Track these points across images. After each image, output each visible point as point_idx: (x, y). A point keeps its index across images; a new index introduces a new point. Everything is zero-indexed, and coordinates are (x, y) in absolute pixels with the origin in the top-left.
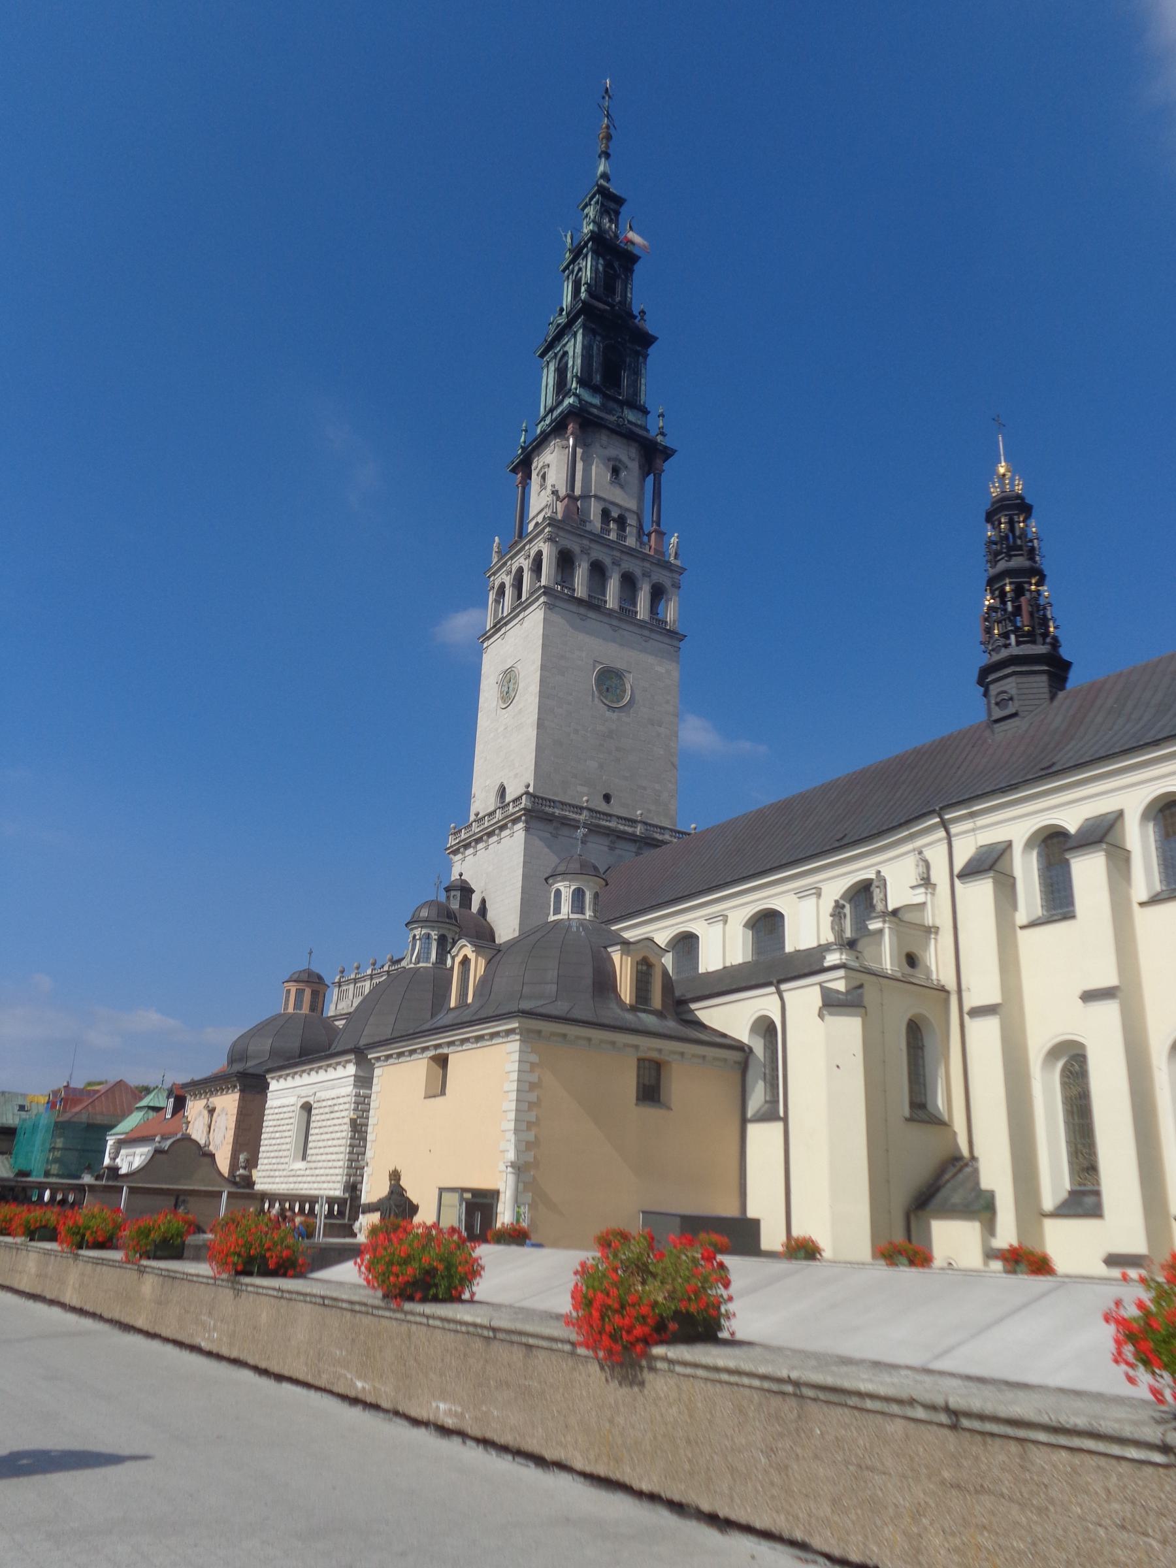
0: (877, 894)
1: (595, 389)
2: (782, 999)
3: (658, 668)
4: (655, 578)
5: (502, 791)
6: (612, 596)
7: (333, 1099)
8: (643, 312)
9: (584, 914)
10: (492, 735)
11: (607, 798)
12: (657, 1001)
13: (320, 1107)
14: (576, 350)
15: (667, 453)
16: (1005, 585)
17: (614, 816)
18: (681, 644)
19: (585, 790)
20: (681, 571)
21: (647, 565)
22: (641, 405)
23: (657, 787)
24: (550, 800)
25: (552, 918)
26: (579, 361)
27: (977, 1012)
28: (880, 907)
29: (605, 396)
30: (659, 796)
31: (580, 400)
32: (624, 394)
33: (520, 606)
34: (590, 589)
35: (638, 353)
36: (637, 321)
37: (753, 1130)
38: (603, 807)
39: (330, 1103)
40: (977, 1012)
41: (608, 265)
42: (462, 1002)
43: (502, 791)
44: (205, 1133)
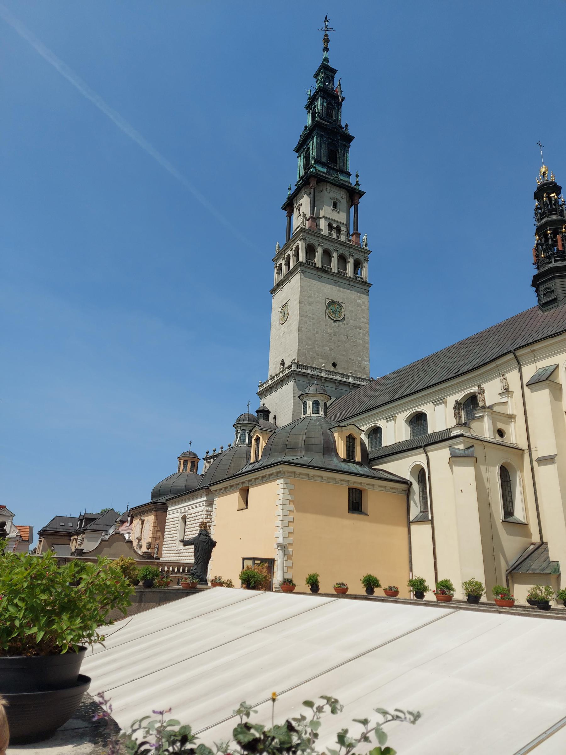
0: (479, 397)
1: (323, 165)
2: (427, 455)
3: (358, 301)
4: (356, 256)
5: (283, 363)
6: (334, 266)
7: (196, 513)
8: (347, 126)
9: (319, 414)
10: (277, 337)
11: (334, 365)
12: (358, 458)
13: (190, 518)
14: (314, 146)
16: (548, 230)
17: (337, 373)
18: (370, 289)
19: (323, 361)
20: (369, 252)
21: (351, 250)
22: (347, 171)
23: (359, 359)
24: (306, 366)
25: (302, 416)
26: (315, 151)
27: (544, 461)
28: (481, 404)
29: (329, 167)
30: (361, 364)
31: (316, 170)
32: (339, 166)
33: (290, 274)
34: (323, 263)
35: (345, 145)
36: (344, 130)
37: (413, 527)
38: (332, 369)
39: (195, 515)
40: (544, 461)
41: (329, 103)
42: (257, 461)
43: (283, 363)
44: (140, 532)
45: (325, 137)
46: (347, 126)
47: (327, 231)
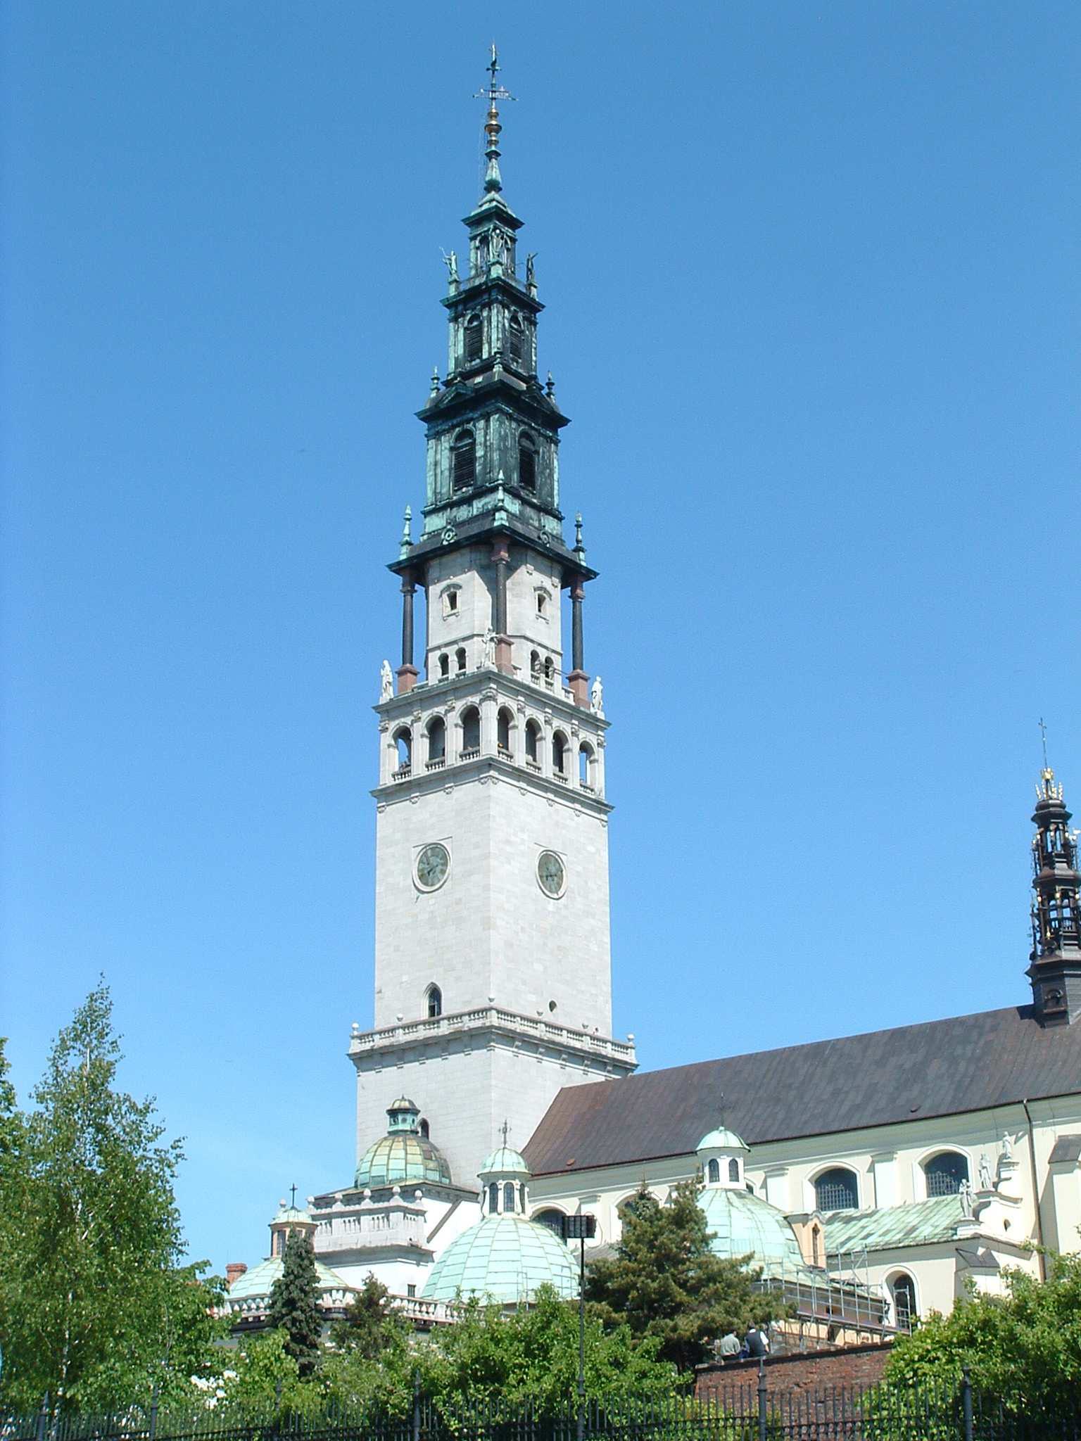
8: (550, 384)
11: (552, 1006)
15: (589, 574)
29: (525, 502)
45: (515, 420)
46: (550, 384)
47: (530, 672)
